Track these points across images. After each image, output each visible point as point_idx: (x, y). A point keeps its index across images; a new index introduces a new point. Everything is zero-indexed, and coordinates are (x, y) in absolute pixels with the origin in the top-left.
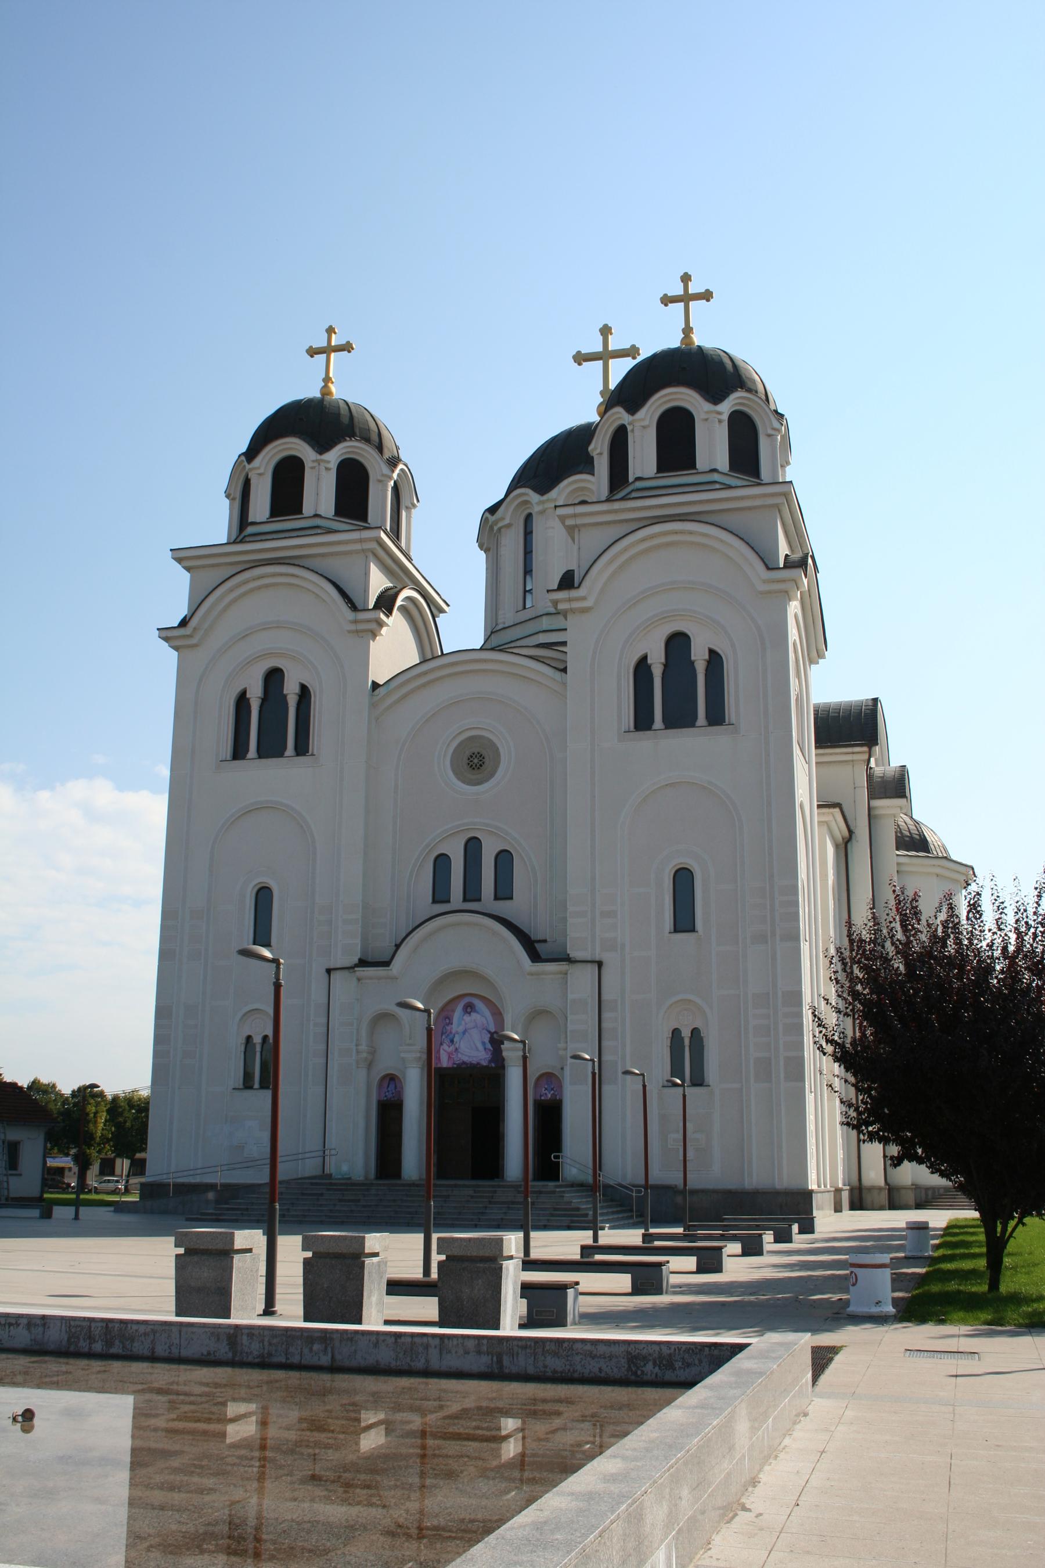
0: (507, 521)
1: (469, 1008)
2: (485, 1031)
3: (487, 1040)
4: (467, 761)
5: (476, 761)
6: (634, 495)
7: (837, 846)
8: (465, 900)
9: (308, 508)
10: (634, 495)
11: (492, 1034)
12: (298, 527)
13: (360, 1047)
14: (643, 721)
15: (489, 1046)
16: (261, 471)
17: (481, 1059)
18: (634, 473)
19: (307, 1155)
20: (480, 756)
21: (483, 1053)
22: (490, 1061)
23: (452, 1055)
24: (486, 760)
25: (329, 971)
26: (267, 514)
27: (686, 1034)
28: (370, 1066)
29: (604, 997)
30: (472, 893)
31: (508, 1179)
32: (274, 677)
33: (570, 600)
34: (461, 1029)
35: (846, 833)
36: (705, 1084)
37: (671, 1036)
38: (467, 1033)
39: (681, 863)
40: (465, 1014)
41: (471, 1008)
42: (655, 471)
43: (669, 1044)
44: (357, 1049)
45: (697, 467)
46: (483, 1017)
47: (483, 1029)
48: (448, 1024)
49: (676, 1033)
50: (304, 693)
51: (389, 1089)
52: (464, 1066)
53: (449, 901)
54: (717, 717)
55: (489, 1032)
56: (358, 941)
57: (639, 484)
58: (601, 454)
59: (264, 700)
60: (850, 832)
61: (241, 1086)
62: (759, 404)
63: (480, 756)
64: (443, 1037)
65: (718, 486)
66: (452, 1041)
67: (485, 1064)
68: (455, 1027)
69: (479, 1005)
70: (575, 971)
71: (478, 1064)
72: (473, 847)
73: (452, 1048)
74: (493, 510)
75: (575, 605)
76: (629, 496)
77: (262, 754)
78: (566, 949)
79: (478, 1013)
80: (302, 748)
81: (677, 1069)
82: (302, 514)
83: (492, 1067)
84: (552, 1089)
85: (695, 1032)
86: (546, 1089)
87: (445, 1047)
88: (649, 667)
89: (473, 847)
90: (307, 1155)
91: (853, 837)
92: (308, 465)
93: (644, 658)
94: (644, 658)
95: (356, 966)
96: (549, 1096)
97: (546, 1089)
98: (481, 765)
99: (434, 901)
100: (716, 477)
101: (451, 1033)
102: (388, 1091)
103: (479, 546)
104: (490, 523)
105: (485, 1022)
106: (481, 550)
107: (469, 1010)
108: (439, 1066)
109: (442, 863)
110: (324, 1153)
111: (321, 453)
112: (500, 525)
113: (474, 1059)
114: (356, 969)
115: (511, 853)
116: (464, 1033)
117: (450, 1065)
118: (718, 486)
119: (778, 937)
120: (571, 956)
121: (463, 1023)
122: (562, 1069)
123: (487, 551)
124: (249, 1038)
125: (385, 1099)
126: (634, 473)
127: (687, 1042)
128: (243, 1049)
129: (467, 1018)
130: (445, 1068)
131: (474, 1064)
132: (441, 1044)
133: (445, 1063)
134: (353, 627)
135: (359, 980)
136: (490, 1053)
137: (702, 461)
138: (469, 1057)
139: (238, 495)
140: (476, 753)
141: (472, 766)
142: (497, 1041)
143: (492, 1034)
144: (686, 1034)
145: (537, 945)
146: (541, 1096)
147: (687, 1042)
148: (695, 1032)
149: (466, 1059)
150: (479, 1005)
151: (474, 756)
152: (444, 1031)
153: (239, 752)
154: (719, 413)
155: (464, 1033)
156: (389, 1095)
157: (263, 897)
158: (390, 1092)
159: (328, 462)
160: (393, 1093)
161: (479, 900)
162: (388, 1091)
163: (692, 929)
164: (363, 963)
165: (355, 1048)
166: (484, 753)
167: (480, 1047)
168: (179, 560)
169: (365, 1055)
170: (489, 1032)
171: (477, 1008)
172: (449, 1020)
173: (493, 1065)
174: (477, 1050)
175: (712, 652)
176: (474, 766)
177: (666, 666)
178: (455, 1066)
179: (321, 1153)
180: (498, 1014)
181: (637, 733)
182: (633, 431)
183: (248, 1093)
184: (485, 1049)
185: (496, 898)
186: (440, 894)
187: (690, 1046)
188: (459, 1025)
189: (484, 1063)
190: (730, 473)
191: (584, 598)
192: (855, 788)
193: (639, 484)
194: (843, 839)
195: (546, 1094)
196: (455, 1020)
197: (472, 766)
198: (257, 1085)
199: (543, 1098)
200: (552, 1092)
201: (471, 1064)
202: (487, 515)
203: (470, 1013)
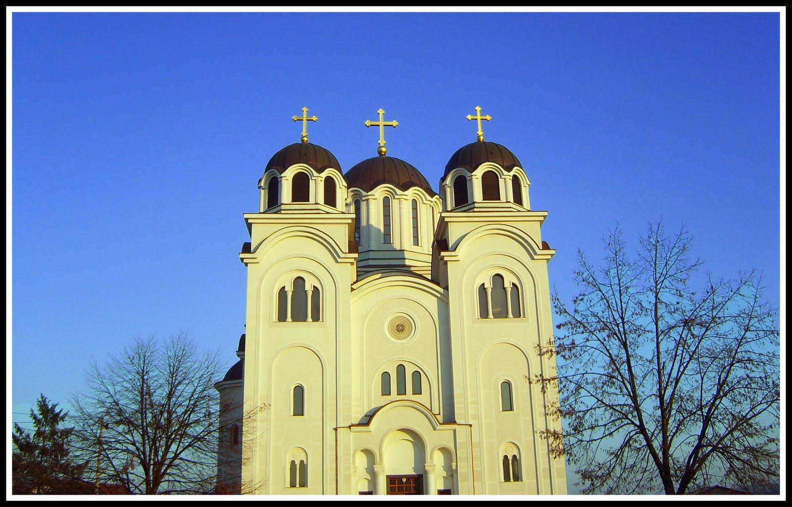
4: (405, 328)
5: (400, 328)
12: (308, 208)
16: (286, 178)
30: (402, 391)
32: (299, 282)
57: (476, 205)
72: (401, 369)
75: (453, 258)
76: (472, 210)
80: (316, 318)
82: (309, 201)
85: (514, 457)
88: (485, 289)
89: (401, 369)
109: (386, 376)
111: (319, 174)
153: (282, 317)
157: (299, 392)
166: (397, 324)
186: (386, 391)
198: (298, 485)
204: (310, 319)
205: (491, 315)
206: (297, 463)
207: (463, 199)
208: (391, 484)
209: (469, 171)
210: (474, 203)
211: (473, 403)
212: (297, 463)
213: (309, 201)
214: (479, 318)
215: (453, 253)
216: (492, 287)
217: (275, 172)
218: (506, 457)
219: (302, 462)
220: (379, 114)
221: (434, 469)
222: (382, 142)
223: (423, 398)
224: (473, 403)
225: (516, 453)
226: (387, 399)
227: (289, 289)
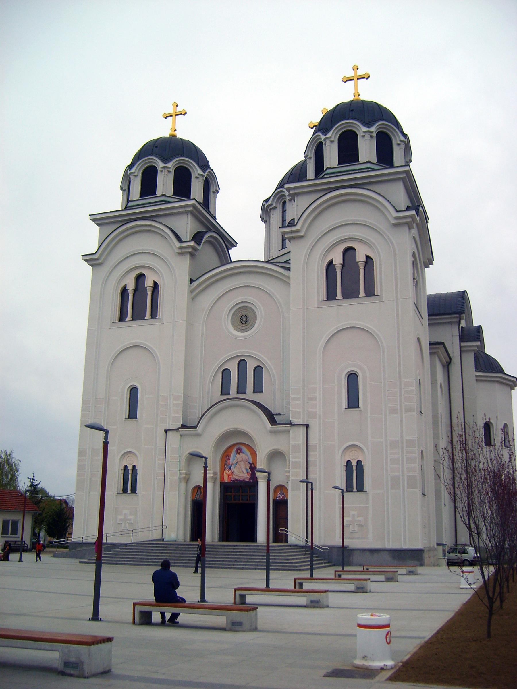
0: (274, 205)
1: (239, 451)
2: (247, 463)
3: (248, 468)
5: (244, 319)
6: (325, 176)
7: (443, 366)
8: (238, 393)
9: (159, 192)
10: (325, 176)
11: (251, 464)
13: (181, 471)
14: (331, 295)
15: (249, 471)
16: (136, 174)
17: (245, 478)
18: (326, 166)
19: (154, 528)
20: (246, 317)
21: (247, 474)
22: (250, 479)
23: (230, 475)
24: (250, 319)
25: (166, 431)
26: (139, 196)
28: (187, 481)
29: (310, 443)
30: (241, 389)
31: (259, 542)
33: (292, 232)
34: (234, 462)
35: (448, 360)
36: (364, 491)
37: (346, 464)
38: (238, 464)
39: (352, 371)
40: (236, 454)
41: (240, 450)
42: (337, 164)
43: (345, 469)
44: (180, 472)
45: (359, 161)
46: (246, 455)
47: (246, 462)
48: (228, 460)
49: (348, 462)
50: (155, 284)
51: (198, 494)
52: (236, 481)
53: (230, 394)
54: (370, 292)
55: (249, 463)
56: (181, 415)
57: (328, 171)
58: (310, 158)
59: (136, 290)
60: (450, 359)
61: (121, 492)
62: (393, 128)
63: (246, 317)
64: (226, 466)
65: (370, 169)
66: (230, 468)
67: (247, 481)
68: (231, 461)
69: (244, 449)
70: (293, 430)
71: (244, 480)
72: (242, 364)
73: (230, 472)
74: (267, 201)
77: (133, 318)
78: (289, 417)
79: (243, 453)
80: (154, 315)
82: (156, 195)
83: (251, 482)
84: (283, 494)
85: (359, 462)
86: (280, 494)
87: (226, 471)
89: (242, 364)
90: (154, 528)
91: (452, 361)
92: (159, 169)
93: (331, 262)
94: (331, 262)
95: (180, 428)
96: (281, 497)
97: (280, 494)
98: (247, 322)
99: (222, 394)
100: (369, 165)
101: (229, 464)
102: (197, 495)
103: (261, 220)
104: (266, 206)
105: (247, 458)
106: (263, 222)
107: (239, 451)
108: (223, 481)
109: (226, 373)
110: (162, 527)
112: (270, 208)
113: (242, 478)
114: (179, 430)
116: (236, 464)
117: (229, 481)
118: (370, 169)
119: (403, 410)
120: (292, 422)
121: (236, 458)
122: (288, 483)
123: (265, 222)
124: (126, 467)
125: (195, 499)
126: (326, 166)
127: (354, 468)
128: (123, 473)
129: (238, 456)
130: (226, 482)
131: (241, 481)
133: (226, 480)
134: (180, 251)
135: (181, 435)
136: (250, 475)
137: (362, 158)
138: (239, 476)
139: (126, 188)
140: (244, 315)
141: (242, 322)
142: (253, 468)
143: (251, 464)
145: (274, 416)
146: (277, 497)
147: (354, 468)
148: (359, 462)
149: (237, 478)
150: (244, 449)
151: (243, 317)
152: (226, 463)
153: (122, 318)
154: (371, 132)
155: (236, 464)
157: (133, 392)
158: (198, 495)
159: (169, 168)
160: (199, 496)
162: (197, 495)
163: (358, 407)
164: (183, 426)
165: (178, 471)
167: (245, 472)
168: (93, 220)
169: (184, 476)
170: (249, 463)
171: (243, 451)
172: (228, 457)
173: (252, 481)
175: (368, 257)
176: (243, 322)
177: (343, 265)
178: (232, 481)
180: (254, 454)
182: (325, 144)
183: (125, 495)
184: (247, 472)
185: (254, 392)
186: (225, 390)
187: (356, 470)
188: (234, 459)
189: (247, 480)
190: (377, 163)
192: (452, 336)
193: (328, 171)
194: (446, 362)
195: (280, 496)
196: (231, 458)
197: (242, 322)
198: (129, 492)
199: (278, 498)
200: (283, 495)
201: (240, 480)
202: (264, 203)
203: (239, 453)
205: (339, 296)
206: (130, 468)
212: (130, 468)
213: (156, 195)
219: (134, 467)
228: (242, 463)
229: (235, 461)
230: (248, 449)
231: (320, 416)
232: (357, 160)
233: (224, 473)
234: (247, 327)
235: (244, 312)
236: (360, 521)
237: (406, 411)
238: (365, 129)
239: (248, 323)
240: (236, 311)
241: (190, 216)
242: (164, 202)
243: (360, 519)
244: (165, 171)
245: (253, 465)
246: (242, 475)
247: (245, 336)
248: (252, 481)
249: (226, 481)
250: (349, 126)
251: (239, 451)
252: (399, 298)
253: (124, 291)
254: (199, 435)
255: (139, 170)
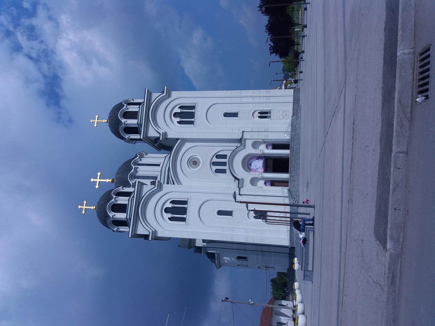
3: (258, 161)
5: (195, 163)
21: (260, 161)
22: (263, 160)
27: (259, 115)
30: (224, 164)
32: (167, 210)
33: (163, 135)
34: (255, 166)
48: (254, 170)
49: (259, 117)
66: (257, 169)
69: (249, 162)
70: (244, 137)
72: (214, 164)
73: (259, 169)
76: (141, 125)
81: (266, 117)
85: (259, 113)
87: (258, 170)
89: (214, 164)
107: (251, 165)
108: (263, 172)
109: (217, 171)
115: (216, 170)
116: (256, 166)
117: (263, 169)
122: (265, 142)
127: (261, 115)
132: (258, 171)
133: (262, 170)
144: (259, 115)
147: (261, 115)
148: (259, 113)
150: (249, 162)
153: (184, 220)
155: (256, 166)
156: (269, 184)
157: (220, 213)
161: (226, 162)
167: (259, 162)
173: (263, 159)
174: (260, 163)
179: (283, 198)
181: (194, 123)
186: (224, 171)
188: (254, 167)
189: (263, 161)
191: (163, 133)
204: (186, 206)
207: (134, 130)
208: (268, 171)
209: (122, 125)
210: (138, 123)
211: (232, 130)
214: (193, 125)
215: (161, 134)
216: (179, 118)
217: (109, 221)
218: (259, 117)
220: (93, 181)
221: (262, 150)
222: (108, 180)
223: (228, 153)
224: (232, 130)
225: (257, 112)
226: (228, 171)
227: (170, 215)
228: (255, 163)
229: (254, 166)
230: (250, 161)
231: (240, 127)
232: (137, 112)
233: (259, 171)
234: (198, 162)
235: (192, 163)
236: (282, 112)
237: (241, 94)
238: (125, 107)
239: (196, 161)
240: (190, 166)
241: (143, 185)
242: (133, 199)
243: (281, 112)
244: (117, 199)
245: (257, 159)
246: (260, 163)
247: (202, 162)
248: (263, 159)
249: (263, 170)
250: (121, 114)
251: (251, 165)
252: (198, 95)
253: (170, 219)
254: (243, 179)
255: (112, 213)
